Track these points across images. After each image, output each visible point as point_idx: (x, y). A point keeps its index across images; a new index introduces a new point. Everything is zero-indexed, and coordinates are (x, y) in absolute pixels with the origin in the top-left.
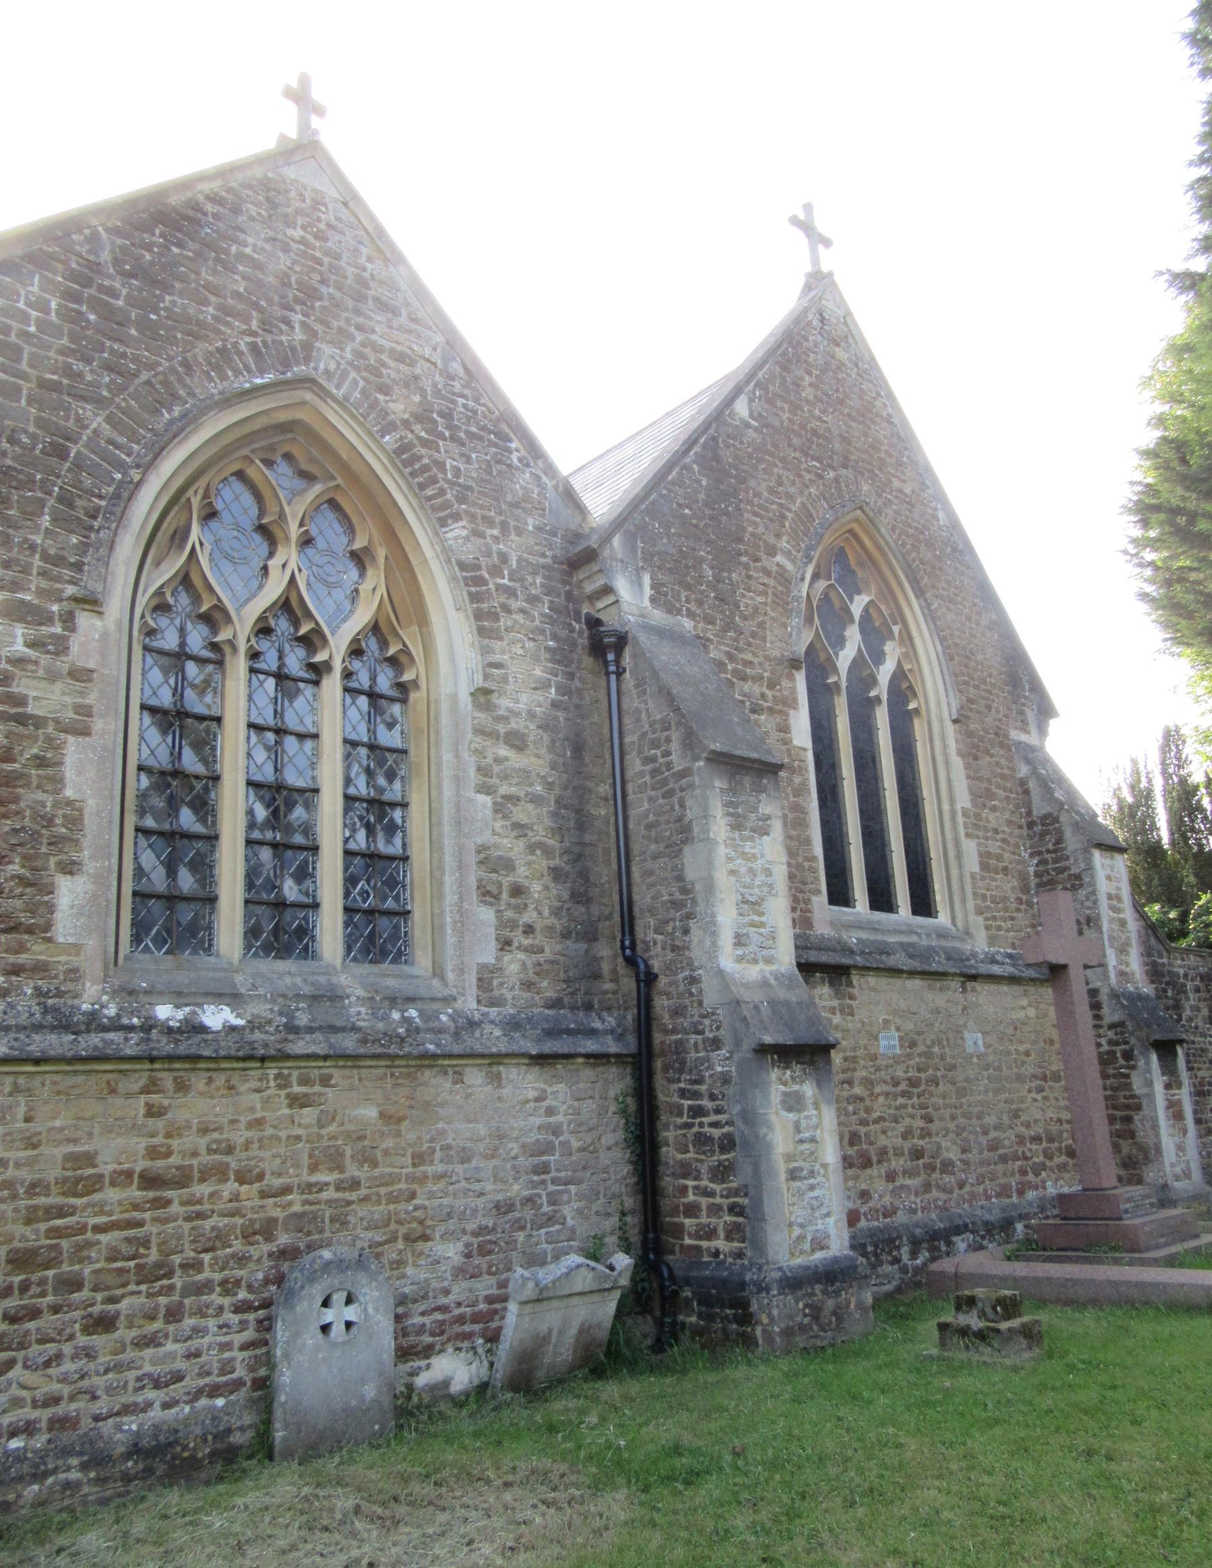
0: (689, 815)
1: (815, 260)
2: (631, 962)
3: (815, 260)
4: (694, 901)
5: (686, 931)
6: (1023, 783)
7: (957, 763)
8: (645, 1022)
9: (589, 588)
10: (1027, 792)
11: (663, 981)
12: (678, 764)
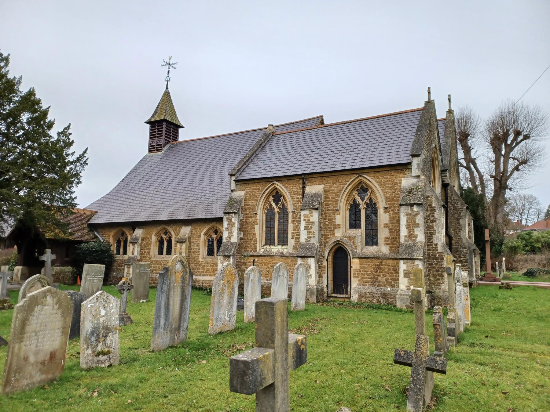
0: (461, 215)
1: (450, 107)
3: (450, 107)
4: (462, 228)
5: (460, 232)
11: (454, 238)
12: (459, 206)
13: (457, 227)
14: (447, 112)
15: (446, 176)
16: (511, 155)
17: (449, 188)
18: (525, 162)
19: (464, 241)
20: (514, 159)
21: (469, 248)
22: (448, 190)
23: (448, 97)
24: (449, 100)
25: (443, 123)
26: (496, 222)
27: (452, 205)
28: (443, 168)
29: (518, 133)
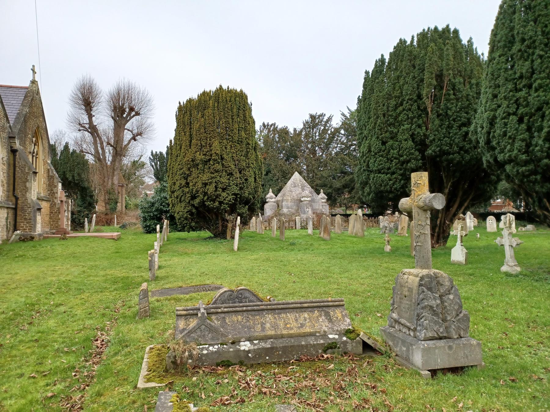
0: (28, 179)
1: (34, 77)
2: (15, 196)
3: (34, 77)
4: (28, 190)
6: (48, 169)
7: (42, 166)
8: (16, 204)
9: (11, 141)
10: (49, 171)
11: (20, 199)
13: (24, 189)
14: (31, 81)
15: (15, 143)
16: (126, 128)
17: (17, 154)
18: (140, 134)
19: (29, 201)
20: (128, 130)
21: (34, 207)
22: (16, 155)
23: (31, 67)
24: (33, 70)
25: (25, 91)
26: (113, 184)
27: (20, 169)
28: (11, 135)
29: (132, 109)
